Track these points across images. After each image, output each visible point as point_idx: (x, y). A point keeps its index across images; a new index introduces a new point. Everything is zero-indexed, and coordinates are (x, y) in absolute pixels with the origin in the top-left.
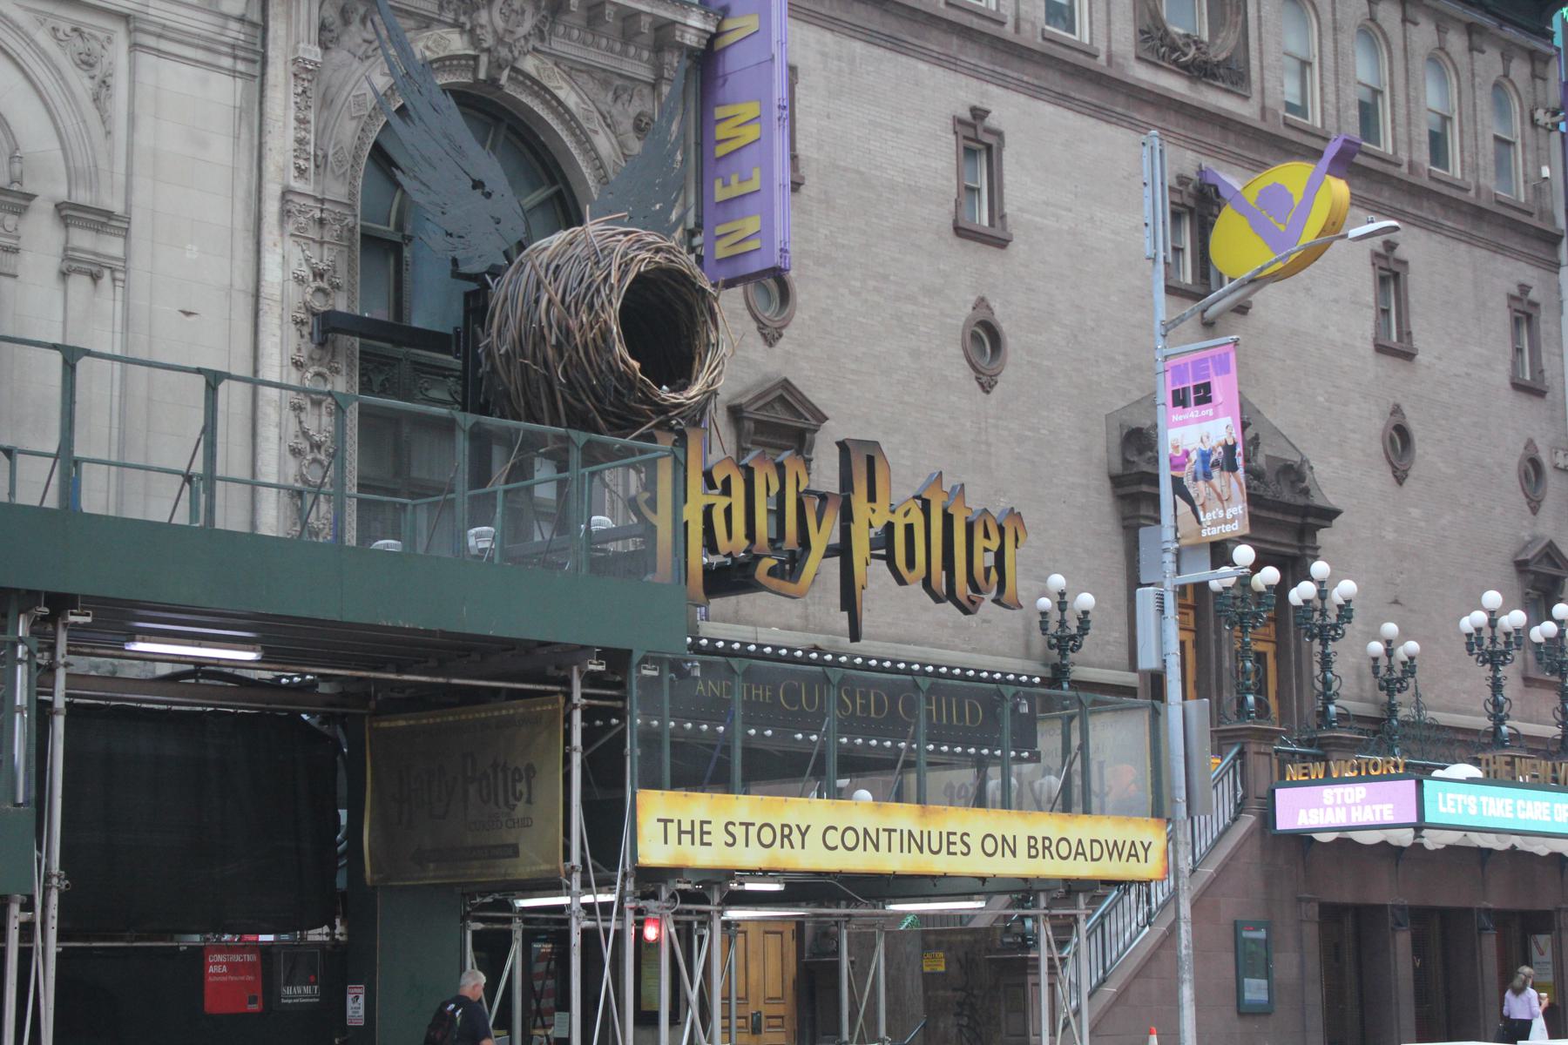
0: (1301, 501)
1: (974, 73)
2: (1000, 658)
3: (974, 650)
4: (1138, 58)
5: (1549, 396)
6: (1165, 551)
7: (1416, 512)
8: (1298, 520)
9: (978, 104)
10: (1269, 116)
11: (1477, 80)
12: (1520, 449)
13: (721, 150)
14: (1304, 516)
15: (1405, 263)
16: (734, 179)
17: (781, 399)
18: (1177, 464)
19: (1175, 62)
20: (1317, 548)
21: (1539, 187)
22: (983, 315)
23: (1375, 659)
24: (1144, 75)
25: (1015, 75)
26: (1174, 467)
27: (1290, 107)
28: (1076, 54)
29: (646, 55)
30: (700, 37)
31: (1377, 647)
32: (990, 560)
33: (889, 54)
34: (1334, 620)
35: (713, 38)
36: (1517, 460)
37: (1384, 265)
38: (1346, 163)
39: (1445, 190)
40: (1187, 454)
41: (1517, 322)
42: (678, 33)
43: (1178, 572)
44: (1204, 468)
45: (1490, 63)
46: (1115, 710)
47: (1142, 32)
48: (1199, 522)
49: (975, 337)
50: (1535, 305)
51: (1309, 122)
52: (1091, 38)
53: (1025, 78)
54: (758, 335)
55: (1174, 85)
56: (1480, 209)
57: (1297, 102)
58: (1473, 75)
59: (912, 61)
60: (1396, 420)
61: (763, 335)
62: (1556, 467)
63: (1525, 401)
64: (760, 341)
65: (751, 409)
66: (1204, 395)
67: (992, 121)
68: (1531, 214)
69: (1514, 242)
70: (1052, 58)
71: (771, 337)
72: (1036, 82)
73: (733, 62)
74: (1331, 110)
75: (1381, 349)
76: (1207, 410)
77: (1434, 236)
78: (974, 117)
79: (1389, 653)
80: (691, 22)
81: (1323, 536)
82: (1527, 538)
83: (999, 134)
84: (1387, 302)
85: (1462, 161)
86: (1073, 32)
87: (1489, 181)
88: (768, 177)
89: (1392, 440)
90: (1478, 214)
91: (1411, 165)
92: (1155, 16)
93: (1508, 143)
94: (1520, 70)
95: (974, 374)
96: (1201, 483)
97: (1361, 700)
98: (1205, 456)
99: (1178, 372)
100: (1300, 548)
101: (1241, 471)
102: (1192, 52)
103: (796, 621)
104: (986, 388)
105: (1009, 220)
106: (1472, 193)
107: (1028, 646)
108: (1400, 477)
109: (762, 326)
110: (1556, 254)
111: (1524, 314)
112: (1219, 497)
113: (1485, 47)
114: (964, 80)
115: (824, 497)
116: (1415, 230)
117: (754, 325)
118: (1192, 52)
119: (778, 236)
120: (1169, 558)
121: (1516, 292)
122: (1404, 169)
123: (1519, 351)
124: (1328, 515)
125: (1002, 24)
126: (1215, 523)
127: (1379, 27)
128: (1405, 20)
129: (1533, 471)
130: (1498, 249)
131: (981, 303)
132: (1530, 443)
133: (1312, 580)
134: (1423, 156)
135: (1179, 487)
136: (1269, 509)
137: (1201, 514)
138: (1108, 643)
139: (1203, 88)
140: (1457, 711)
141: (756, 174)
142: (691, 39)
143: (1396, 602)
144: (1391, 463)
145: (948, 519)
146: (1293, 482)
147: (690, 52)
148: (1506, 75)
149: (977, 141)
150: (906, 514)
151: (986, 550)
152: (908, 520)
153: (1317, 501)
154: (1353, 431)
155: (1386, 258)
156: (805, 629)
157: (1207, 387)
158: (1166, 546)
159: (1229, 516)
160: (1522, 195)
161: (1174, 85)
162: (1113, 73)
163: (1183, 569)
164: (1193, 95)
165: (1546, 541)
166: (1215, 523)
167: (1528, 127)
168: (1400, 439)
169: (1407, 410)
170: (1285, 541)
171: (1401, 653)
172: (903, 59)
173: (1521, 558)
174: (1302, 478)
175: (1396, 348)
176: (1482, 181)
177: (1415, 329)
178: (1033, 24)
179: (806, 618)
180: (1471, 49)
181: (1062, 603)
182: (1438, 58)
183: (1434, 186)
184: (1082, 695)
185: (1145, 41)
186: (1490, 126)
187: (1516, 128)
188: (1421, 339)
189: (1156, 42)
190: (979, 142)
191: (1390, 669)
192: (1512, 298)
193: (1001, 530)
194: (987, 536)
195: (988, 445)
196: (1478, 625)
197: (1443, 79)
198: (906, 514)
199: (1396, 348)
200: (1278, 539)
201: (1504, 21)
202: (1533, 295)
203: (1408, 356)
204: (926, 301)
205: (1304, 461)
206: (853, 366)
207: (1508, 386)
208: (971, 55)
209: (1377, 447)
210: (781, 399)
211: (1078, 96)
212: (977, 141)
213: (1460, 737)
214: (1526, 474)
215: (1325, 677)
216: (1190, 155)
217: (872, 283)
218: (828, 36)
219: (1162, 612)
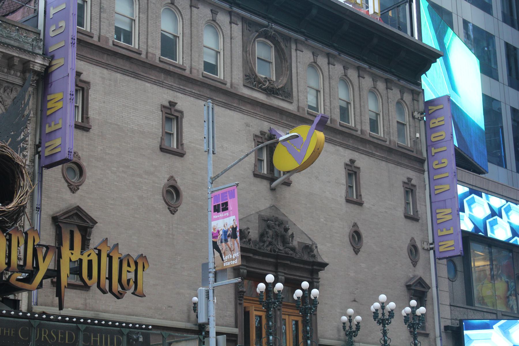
0: (311, 260)
1: (171, 88)
2: (174, 322)
3: (164, 319)
4: (244, 86)
5: (420, 221)
6: (210, 272)
7: (363, 265)
8: (310, 267)
9: (172, 100)
10: (300, 110)
11: (389, 100)
12: (409, 242)
13: (49, 112)
14: (312, 266)
15: (359, 168)
16: (53, 124)
17: (76, 214)
18: (215, 236)
19: (260, 88)
20: (319, 279)
21: (416, 141)
22: (172, 183)
23: (344, 323)
24: (247, 92)
25: (189, 90)
26: (213, 237)
27: (310, 107)
28: (217, 83)
29: (19, 74)
30: (42, 67)
31: (345, 318)
32: (132, 276)
33: (132, 79)
34: (387, 317)
35: (48, 68)
36: (407, 245)
37: (350, 168)
38: (323, 125)
39: (376, 141)
40: (218, 231)
41: (407, 193)
42: (31, 65)
43: (215, 281)
44: (225, 237)
45: (395, 94)
46: (186, 340)
47: (246, 76)
48: (223, 260)
49: (168, 192)
50: (414, 186)
51: (350, 125)
52: (224, 77)
53: (194, 91)
54: (68, 188)
55: (261, 97)
56: (390, 149)
57: (315, 106)
58: (388, 98)
59: (144, 83)
60: (355, 229)
61: (70, 188)
62: (423, 249)
63: (410, 223)
64: (69, 191)
65: (62, 218)
66: (225, 207)
67: (178, 107)
68: (413, 152)
69: (405, 162)
70: (205, 83)
71: (73, 189)
72: (198, 93)
73: (56, 76)
74: (328, 108)
75: (348, 201)
76: (226, 213)
77: (372, 158)
78: (170, 105)
79: (350, 321)
80: (37, 61)
81: (321, 274)
82: (411, 276)
83: (181, 112)
84: (352, 183)
85: (384, 130)
86: (217, 75)
87: (395, 138)
88: (64, 123)
89: (353, 236)
90: (390, 150)
91: (362, 131)
92: (252, 70)
93: (404, 125)
94: (408, 97)
95: (167, 207)
96: (223, 244)
97: (339, 340)
98: (225, 232)
99: (216, 198)
100: (312, 279)
101: (238, 238)
102: (267, 84)
103: (80, 306)
104: (173, 212)
105: (185, 146)
106: (388, 143)
107: (189, 317)
108: (357, 251)
109: (69, 185)
110: (423, 167)
111: (409, 189)
112: (230, 249)
113: (393, 88)
114: (166, 91)
115: (47, 247)
116: (363, 156)
117: (66, 184)
118: (267, 84)
119: (67, 146)
120: (211, 275)
121: (406, 181)
122: (359, 132)
123: (408, 204)
124: (324, 265)
125: (185, 70)
126: (229, 260)
127: (348, 78)
128: (359, 76)
130: (398, 164)
131: (172, 178)
132: (412, 239)
134: (367, 128)
135: (215, 246)
136: (297, 263)
137: (224, 257)
138: (226, 316)
139: (272, 98)
141: (60, 122)
142: (37, 68)
143: (355, 301)
144: (352, 246)
145: (110, 258)
146: (309, 253)
147: (36, 72)
148: (402, 99)
149: (171, 115)
150: (89, 255)
151: (128, 271)
152: (90, 258)
153: (319, 260)
154: (336, 233)
155: (351, 166)
156: (85, 309)
157: (226, 204)
158: (210, 270)
159: (234, 257)
160: (409, 144)
161: (261, 97)
162: (232, 91)
163: (217, 280)
164: (268, 101)
165: (418, 277)
166: (229, 260)
167: (411, 119)
168: (356, 237)
170: (306, 276)
171: (355, 322)
172: (139, 81)
173: (409, 284)
174: (312, 251)
175: (355, 201)
176: (392, 138)
177: (363, 194)
178: (198, 71)
179: (86, 305)
180: (387, 88)
182: (374, 91)
183: (372, 139)
184: (164, 332)
185: (247, 79)
186: (395, 117)
187: (407, 119)
188: (366, 198)
189: (251, 79)
190: (173, 115)
191: (351, 327)
192: (404, 183)
193: (136, 263)
194: (129, 265)
195: (173, 235)
196: (376, 308)
197: (376, 99)
198: (89, 255)
199: (355, 201)
200: (302, 275)
201: (400, 78)
202: (413, 182)
203: (360, 204)
204: (146, 177)
205: (313, 243)
206: (112, 202)
208: (170, 81)
209: (347, 239)
210: (76, 214)
211: (216, 99)
212: (171, 115)
214: (411, 251)
215: (384, 339)
216: (266, 124)
217: (121, 169)
218: (105, 71)
219: (208, 298)
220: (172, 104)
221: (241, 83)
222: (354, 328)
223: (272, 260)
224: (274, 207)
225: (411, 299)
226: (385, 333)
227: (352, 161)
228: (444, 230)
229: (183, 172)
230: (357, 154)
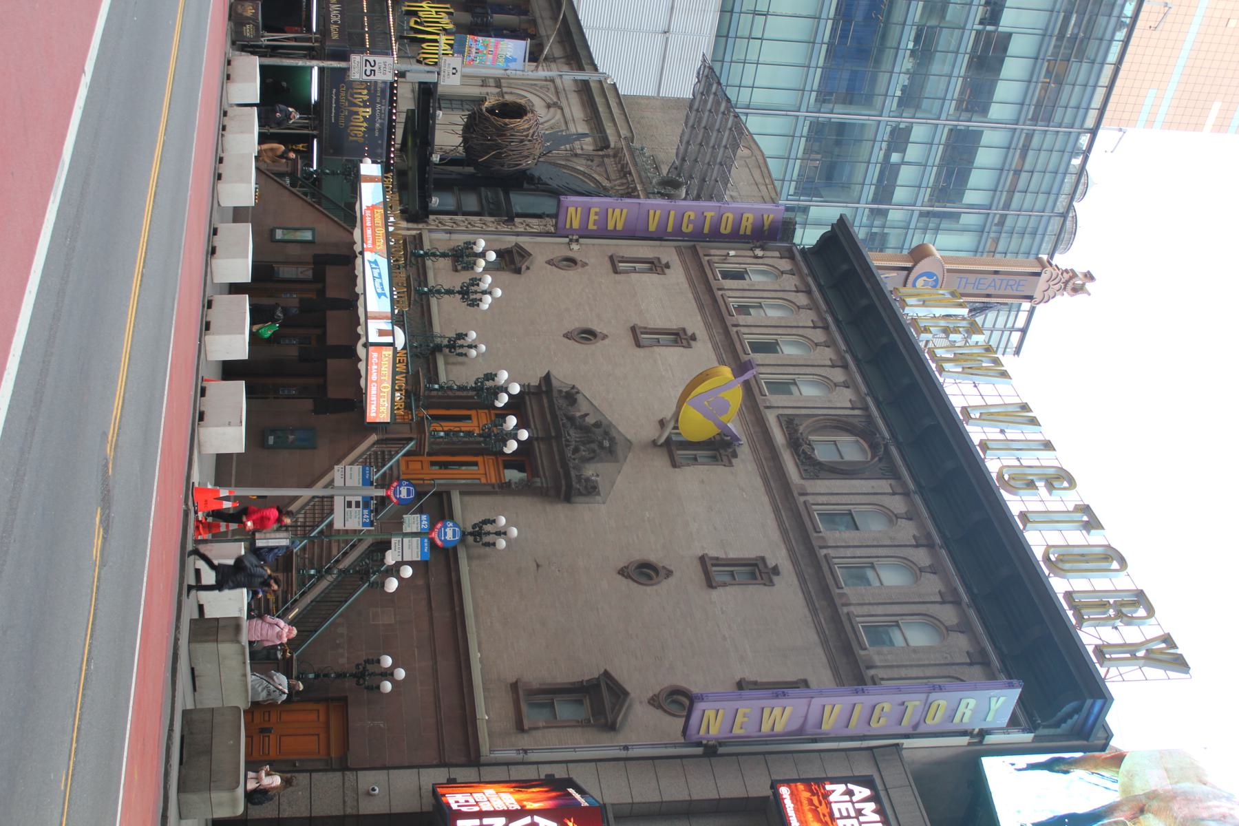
90: (835, 618)
108: (623, 572)
116: (800, 595)
129: (679, 700)
140: (476, 616)
143: (538, 566)
168: (645, 572)
169: (672, 580)
181: (501, 533)
207: (737, 678)
213: (457, 609)
220: (693, 338)
221: (780, 411)
222: (486, 539)
223: (545, 400)
226: (449, 292)
227: (776, 571)
229: (617, 345)
230: (796, 582)
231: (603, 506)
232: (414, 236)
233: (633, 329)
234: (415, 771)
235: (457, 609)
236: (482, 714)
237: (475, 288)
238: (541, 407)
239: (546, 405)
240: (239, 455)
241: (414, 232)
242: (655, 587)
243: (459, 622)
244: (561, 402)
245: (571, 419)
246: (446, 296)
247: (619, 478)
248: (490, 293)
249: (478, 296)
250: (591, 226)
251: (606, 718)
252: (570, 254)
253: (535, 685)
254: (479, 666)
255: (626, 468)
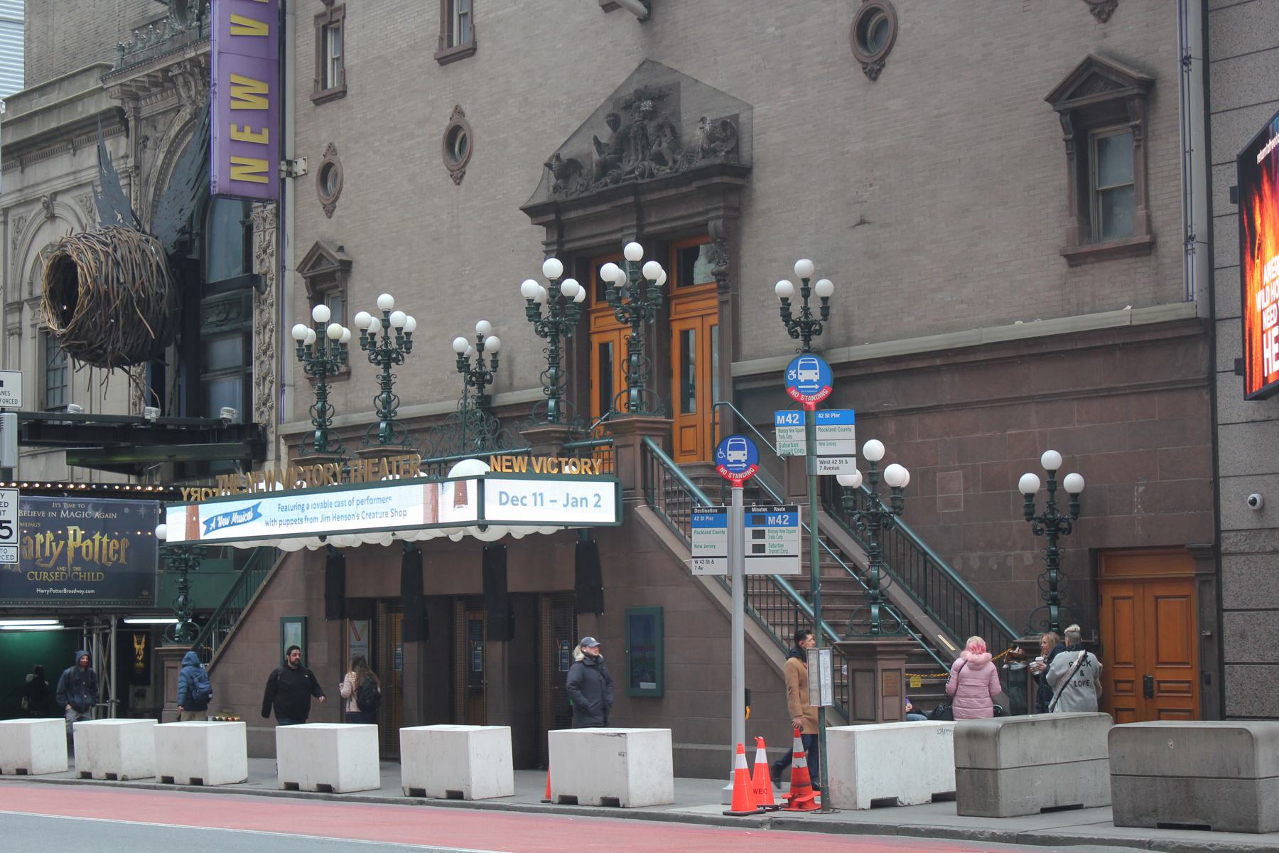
79: (806, 292)
108: (873, 72)
133: (329, 323)
140: (950, 329)
143: (862, 222)
154: (809, 47)
181: (806, 288)
195: (458, 227)
200: (690, 211)
213: (938, 362)
222: (816, 313)
223: (573, 214)
224: (647, 65)
225: (548, 255)
226: (387, 384)
228: (248, 129)
231: (758, 110)
232: (290, 447)
233: (443, 61)
234: (1221, 431)
235: (938, 362)
236: (1123, 316)
237: (378, 339)
238: (584, 221)
239: (581, 213)
240: (674, 740)
241: (284, 449)
242: (900, 14)
243: (960, 359)
244: (575, 185)
245: (604, 168)
246: (394, 389)
247: (708, 81)
248: (387, 313)
249: (393, 334)
250: (264, 138)
251: (1132, 97)
252: (314, 176)
253: (1073, 223)
254: (1038, 322)
255: (690, 70)
